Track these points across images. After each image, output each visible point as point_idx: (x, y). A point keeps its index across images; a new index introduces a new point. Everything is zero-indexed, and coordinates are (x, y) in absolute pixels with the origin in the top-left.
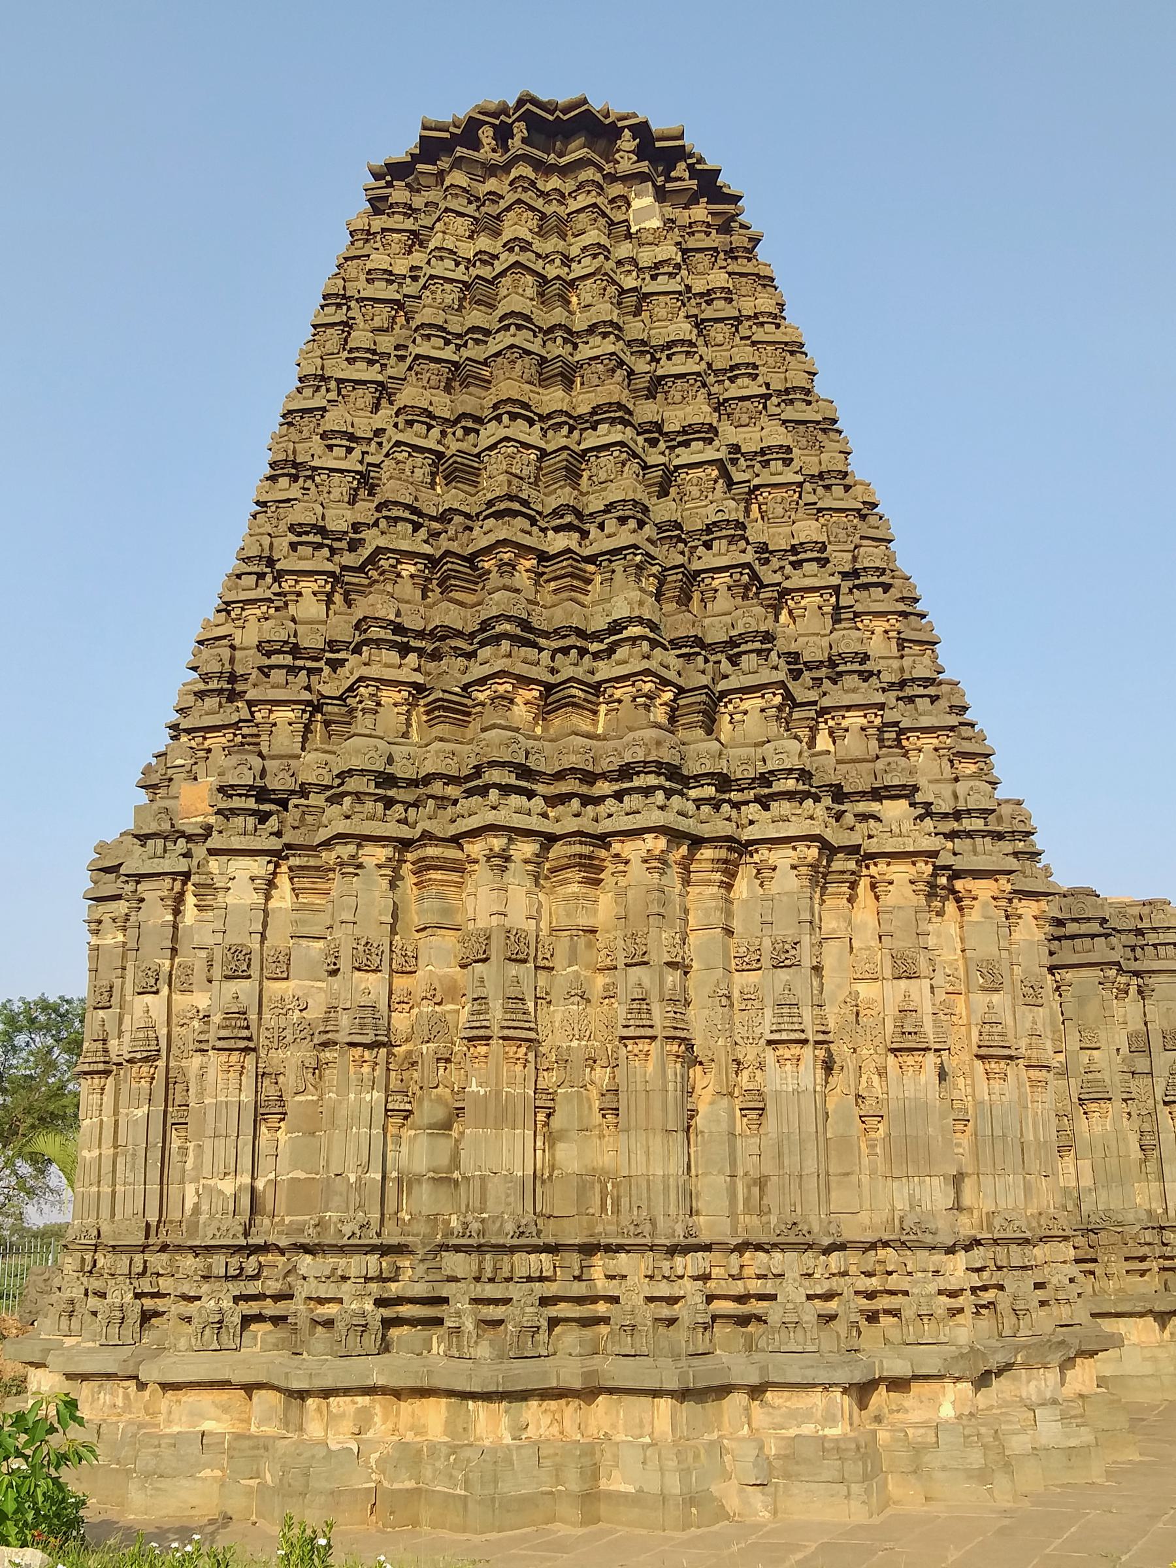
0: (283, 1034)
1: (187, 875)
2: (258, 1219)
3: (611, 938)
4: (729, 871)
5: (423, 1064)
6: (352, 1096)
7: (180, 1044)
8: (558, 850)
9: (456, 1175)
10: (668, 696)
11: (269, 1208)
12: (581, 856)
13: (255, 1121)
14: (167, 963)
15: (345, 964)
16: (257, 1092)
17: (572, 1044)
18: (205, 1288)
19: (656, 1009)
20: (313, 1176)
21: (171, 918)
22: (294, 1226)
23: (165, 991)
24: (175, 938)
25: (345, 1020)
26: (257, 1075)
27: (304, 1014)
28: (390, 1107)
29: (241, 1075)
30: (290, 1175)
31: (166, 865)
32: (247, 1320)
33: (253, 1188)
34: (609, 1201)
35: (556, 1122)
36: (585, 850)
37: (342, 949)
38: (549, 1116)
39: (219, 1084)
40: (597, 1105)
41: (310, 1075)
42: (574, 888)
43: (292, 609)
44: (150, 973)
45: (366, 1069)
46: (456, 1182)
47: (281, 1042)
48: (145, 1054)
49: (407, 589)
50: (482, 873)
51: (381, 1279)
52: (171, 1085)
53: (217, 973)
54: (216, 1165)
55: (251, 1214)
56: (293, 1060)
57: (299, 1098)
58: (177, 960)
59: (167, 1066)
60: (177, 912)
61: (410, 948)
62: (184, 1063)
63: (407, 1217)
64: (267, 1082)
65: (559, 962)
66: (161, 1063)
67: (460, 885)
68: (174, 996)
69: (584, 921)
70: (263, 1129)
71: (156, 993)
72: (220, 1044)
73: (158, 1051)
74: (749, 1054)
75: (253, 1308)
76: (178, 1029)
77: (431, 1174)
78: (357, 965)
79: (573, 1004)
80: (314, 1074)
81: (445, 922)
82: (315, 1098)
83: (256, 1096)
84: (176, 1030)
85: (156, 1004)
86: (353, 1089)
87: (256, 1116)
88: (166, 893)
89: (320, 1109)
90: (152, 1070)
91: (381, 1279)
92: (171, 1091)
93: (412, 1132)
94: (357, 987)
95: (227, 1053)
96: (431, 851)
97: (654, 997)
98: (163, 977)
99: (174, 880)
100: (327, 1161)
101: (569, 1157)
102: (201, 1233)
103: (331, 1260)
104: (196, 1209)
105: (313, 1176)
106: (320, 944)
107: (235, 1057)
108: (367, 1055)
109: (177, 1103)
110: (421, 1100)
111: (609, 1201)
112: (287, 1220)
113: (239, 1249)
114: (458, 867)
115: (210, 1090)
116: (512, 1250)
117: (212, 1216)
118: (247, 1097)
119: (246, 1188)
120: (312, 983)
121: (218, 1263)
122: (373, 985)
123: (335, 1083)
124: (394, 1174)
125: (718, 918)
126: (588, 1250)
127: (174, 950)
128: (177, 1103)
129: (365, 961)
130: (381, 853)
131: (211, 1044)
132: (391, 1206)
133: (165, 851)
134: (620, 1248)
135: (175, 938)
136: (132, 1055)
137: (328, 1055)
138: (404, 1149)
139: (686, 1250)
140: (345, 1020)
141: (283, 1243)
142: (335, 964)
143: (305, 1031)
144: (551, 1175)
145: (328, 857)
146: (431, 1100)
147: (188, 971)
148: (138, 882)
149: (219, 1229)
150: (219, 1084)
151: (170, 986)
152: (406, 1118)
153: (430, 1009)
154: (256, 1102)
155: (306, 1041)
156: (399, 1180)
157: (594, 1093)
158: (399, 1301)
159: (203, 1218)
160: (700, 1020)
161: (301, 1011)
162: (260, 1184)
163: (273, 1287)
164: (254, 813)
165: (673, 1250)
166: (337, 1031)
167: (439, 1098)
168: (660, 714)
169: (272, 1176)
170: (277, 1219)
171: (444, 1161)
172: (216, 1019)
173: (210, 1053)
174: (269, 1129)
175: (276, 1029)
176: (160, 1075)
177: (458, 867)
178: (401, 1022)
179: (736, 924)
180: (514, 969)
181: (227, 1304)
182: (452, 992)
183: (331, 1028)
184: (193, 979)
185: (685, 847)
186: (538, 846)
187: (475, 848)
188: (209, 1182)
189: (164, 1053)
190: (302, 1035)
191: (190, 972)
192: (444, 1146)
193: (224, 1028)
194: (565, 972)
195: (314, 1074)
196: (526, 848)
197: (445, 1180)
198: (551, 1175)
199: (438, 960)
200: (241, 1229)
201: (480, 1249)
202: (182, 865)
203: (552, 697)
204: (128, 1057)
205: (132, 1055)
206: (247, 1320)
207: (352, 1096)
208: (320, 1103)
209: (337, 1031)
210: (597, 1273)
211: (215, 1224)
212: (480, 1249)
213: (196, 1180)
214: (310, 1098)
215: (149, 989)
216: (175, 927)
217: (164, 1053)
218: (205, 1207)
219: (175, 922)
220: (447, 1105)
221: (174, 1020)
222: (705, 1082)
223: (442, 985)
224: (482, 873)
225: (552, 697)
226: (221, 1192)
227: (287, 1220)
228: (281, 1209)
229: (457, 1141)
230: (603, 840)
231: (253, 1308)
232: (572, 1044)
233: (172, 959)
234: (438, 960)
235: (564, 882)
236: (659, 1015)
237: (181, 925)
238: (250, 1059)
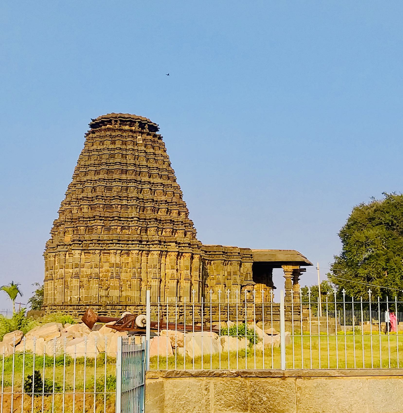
3: (131, 265)
4: (148, 254)
10: (140, 228)
15: (93, 267)
18: (73, 310)
19: (136, 274)
32: (79, 315)
42: (125, 257)
43: (83, 211)
47: (83, 277)
49: (101, 209)
50: (112, 255)
51: (98, 309)
53: (74, 267)
65: (123, 267)
67: (110, 256)
69: (127, 262)
74: (149, 280)
75: (80, 313)
91: (98, 309)
97: (136, 273)
101: (124, 294)
103: (92, 307)
113: (77, 305)
114: (109, 253)
116: (116, 305)
118: (78, 285)
121: (75, 307)
125: (146, 261)
126: (126, 306)
130: (98, 251)
132: (99, 300)
134: (131, 305)
139: (139, 306)
140: (93, 275)
141: (84, 304)
143: (87, 276)
145: (91, 251)
158: (101, 312)
160: (143, 276)
163: (83, 310)
165: (138, 306)
168: (139, 231)
172: (74, 274)
177: (109, 253)
178: (101, 275)
179: (148, 262)
180: (117, 268)
181: (77, 312)
182: (108, 271)
187: (112, 251)
192: (107, 292)
194: (124, 269)
196: (119, 251)
197: (107, 297)
199: (106, 267)
201: (112, 305)
203: (123, 228)
206: (79, 315)
210: (127, 309)
212: (112, 305)
222: (143, 284)
225: (123, 228)
228: (83, 300)
230: (130, 250)
231: (80, 313)
234: (106, 267)
236: (137, 275)
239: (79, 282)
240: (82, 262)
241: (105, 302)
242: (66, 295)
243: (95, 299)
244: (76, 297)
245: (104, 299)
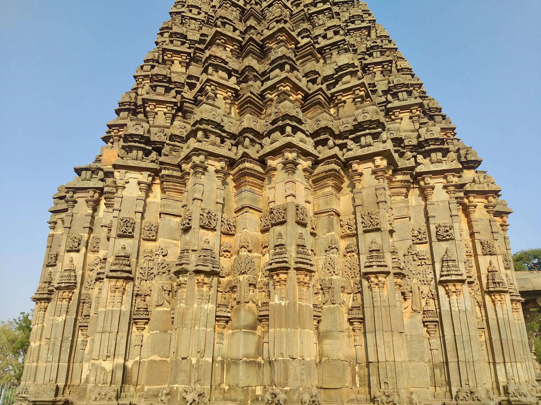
0: (151, 272)
1: (101, 189)
2: (127, 387)
5: (240, 287)
6: (196, 306)
7: (89, 280)
8: (320, 168)
9: (260, 359)
11: (134, 379)
12: (335, 170)
13: (129, 323)
14: (86, 235)
15: (195, 224)
16: (132, 305)
17: (333, 277)
20: (165, 359)
21: (91, 212)
22: (150, 393)
23: (83, 250)
24: (92, 222)
25: (193, 257)
26: (133, 295)
27: (165, 258)
28: (219, 314)
29: (123, 294)
30: (150, 358)
31: (91, 184)
33: (125, 367)
34: (357, 378)
35: (322, 327)
36: (337, 168)
37: (193, 215)
38: (318, 323)
39: (109, 301)
40: (346, 317)
41: (166, 295)
44: (75, 240)
45: (205, 289)
46: (259, 365)
47: (150, 276)
48: (67, 284)
50: (280, 175)
52: (81, 304)
53: (113, 233)
54: (102, 350)
55: (122, 383)
56: (157, 286)
57: (160, 309)
58: (92, 235)
59: (80, 292)
60: (95, 210)
61: (232, 221)
62: (90, 292)
63: (227, 388)
64: (139, 299)
66: (77, 291)
67: (261, 187)
68: (88, 254)
70: (134, 329)
71: (78, 251)
72: (111, 274)
73: (76, 283)
76: (89, 272)
77: (245, 359)
78: (202, 224)
79: (333, 253)
80: (169, 294)
81: (254, 205)
82: (168, 309)
83: (131, 308)
84: (88, 273)
85: (77, 258)
86: (196, 301)
87: (130, 320)
88: (90, 198)
89: (172, 316)
90: (70, 294)
92: (81, 307)
93: (230, 332)
94: (202, 238)
95: (115, 280)
96: (247, 165)
98: (83, 243)
99: (95, 192)
100: (177, 349)
102: (87, 396)
104: (87, 381)
105: (165, 359)
106: (178, 219)
107: (120, 283)
108: (206, 280)
109: (84, 314)
110: (238, 311)
111: (357, 378)
112: (146, 388)
115: (102, 302)
117: (96, 385)
118: (126, 308)
119: (120, 366)
120: (171, 241)
122: (212, 238)
123: (184, 297)
124: (219, 358)
127: (91, 229)
128: (84, 314)
129: (207, 223)
130: (219, 165)
131: (105, 275)
133: (91, 177)
135: (92, 222)
136: (59, 285)
137: (182, 279)
138: (225, 342)
140: (193, 257)
142: (188, 224)
144: (320, 361)
146: (245, 310)
147: (98, 241)
148: (74, 193)
149: (99, 394)
150: (109, 301)
151: (87, 247)
152: (227, 322)
153: (246, 253)
154: (131, 312)
155: (165, 275)
156: (222, 363)
157: (344, 309)
159: (90, 386)
161: (164, 256)
162: (129, 364)
164: (143, 149)
166: (188, 264)
167: (250, 309)
169: (138, 359)
170: (139, 387)
171: (252, 350)
172: (111, 260)
173: (105, 280)
174: (138, 329)
175: (147, 268)
176: (75, 298)
183: (184, 261)
184: (100, 245)
185: (391, 171)
186: (311, 163)
188: (96, 362)
189: (78, 285)
190: (163, 270)
191: (99, 241)
192: (253, 340)
193: (114, 265)
195: (169, 294)
196: (305, 163)
198: (320, 361)
200: (114, 394)
202: (100, 184)
204: (56, 285)
205: (59, 285)
207: (196, 306)
208: (172, 312)
209: (188, 264)
211: (97, 390)
213: (88, 361)
214: (165, 309)
215: (74, 249)
216: (93, 217)
217: (78, 285)
218: (92, 379)
219: (93, 214)
220: (254, 314)
221: (87, 267)
223: (252, 241)
224: (280, 175)
226: (103, 369)
227: (146, 388)
229: (259, 337)
232: (333, 277)
233: (89, 234)
234: (250, 226)
235: (322, 187)
237: (96, 217)
238: (129, 286)
239: (127, 298)
240: (151, 217)
241: (246, 389)
242: (78, 357)
243: (195, 375)
244: (108, 365)
245: (243, 376)
